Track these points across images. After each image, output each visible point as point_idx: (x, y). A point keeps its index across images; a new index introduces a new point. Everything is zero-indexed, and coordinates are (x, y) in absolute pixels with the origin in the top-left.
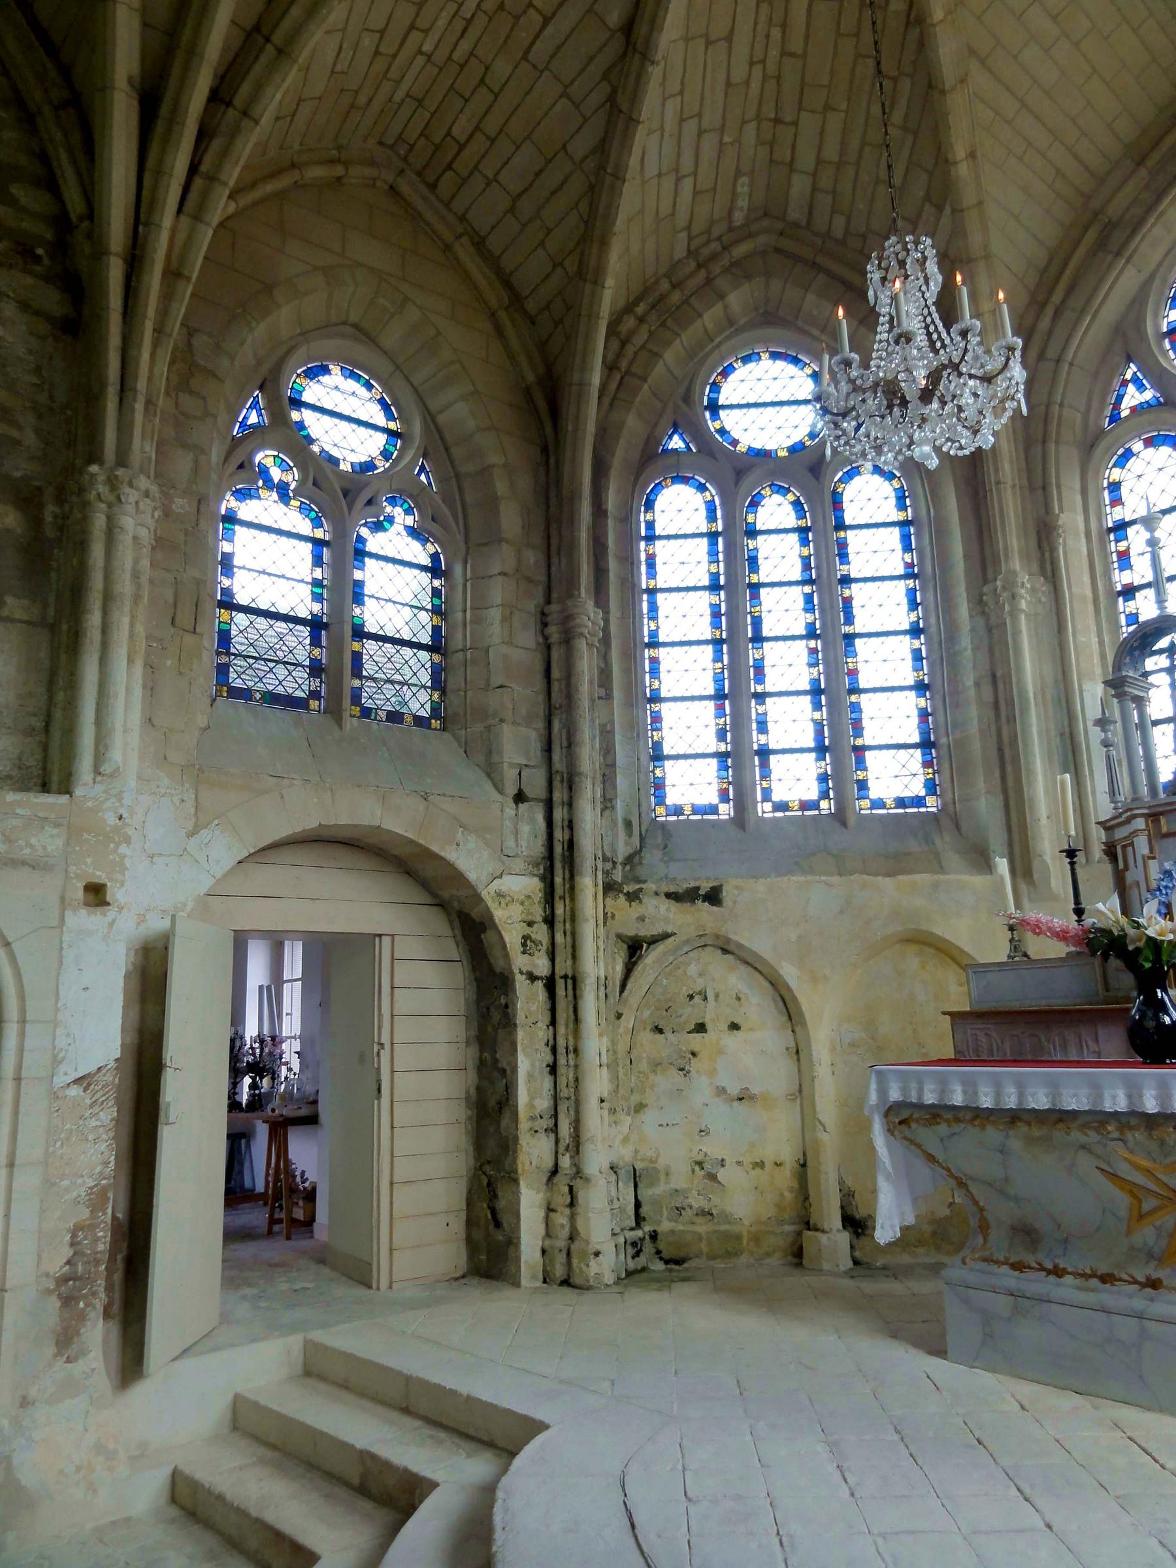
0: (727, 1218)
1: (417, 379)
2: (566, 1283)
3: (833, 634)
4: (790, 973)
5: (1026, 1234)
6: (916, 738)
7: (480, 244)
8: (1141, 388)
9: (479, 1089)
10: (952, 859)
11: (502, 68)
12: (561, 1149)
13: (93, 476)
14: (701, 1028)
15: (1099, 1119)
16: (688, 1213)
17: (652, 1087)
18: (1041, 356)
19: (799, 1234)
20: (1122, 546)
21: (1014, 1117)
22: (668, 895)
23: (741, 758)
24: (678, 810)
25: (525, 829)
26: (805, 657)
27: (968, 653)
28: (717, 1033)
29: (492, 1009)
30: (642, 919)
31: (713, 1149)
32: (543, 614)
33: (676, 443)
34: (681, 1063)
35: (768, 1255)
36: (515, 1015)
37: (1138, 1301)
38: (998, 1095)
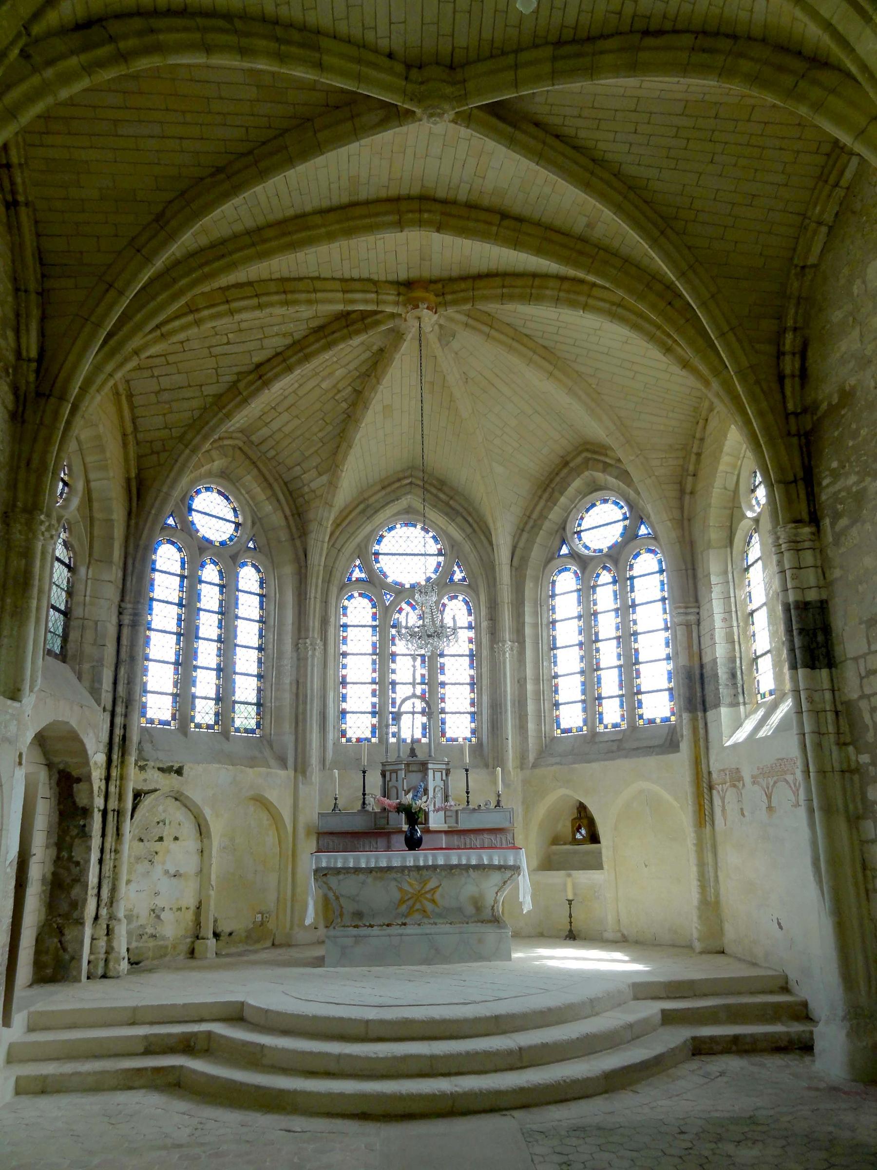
0: (164, 938)
1: (88, 459)
2: (104, 976)
3: (227, 642)
4: (208, 812)
5: (359, 915)
6: (255, 701)
7: (130, 396)
8: (361, 571)
9: (54, 874)
10: (272, 762)
11: (195, 344)
12: (103, 904)
13: (42, 522)
14: (161, 839)
15: (403, 869)
16: (145, 937)
17: (135, 871)
18: (333, 545)
19: (193, 942)
20: (345, 634)
21: (370, 870)
22: (159, 769)
23: (183, 699)
24: (151, 721)
25: (105, 726)
26: (215, 652)
27: (289, 667)
28: (168, 842)
29: (71, 827)
30: (145, 780)
31: (160, 902)
32: (120, 607)
33: (171, 521)
34: (150, 857)
35: (179, 954)
36: (91, 831)
37: (401, 930)
38: (368, 862)
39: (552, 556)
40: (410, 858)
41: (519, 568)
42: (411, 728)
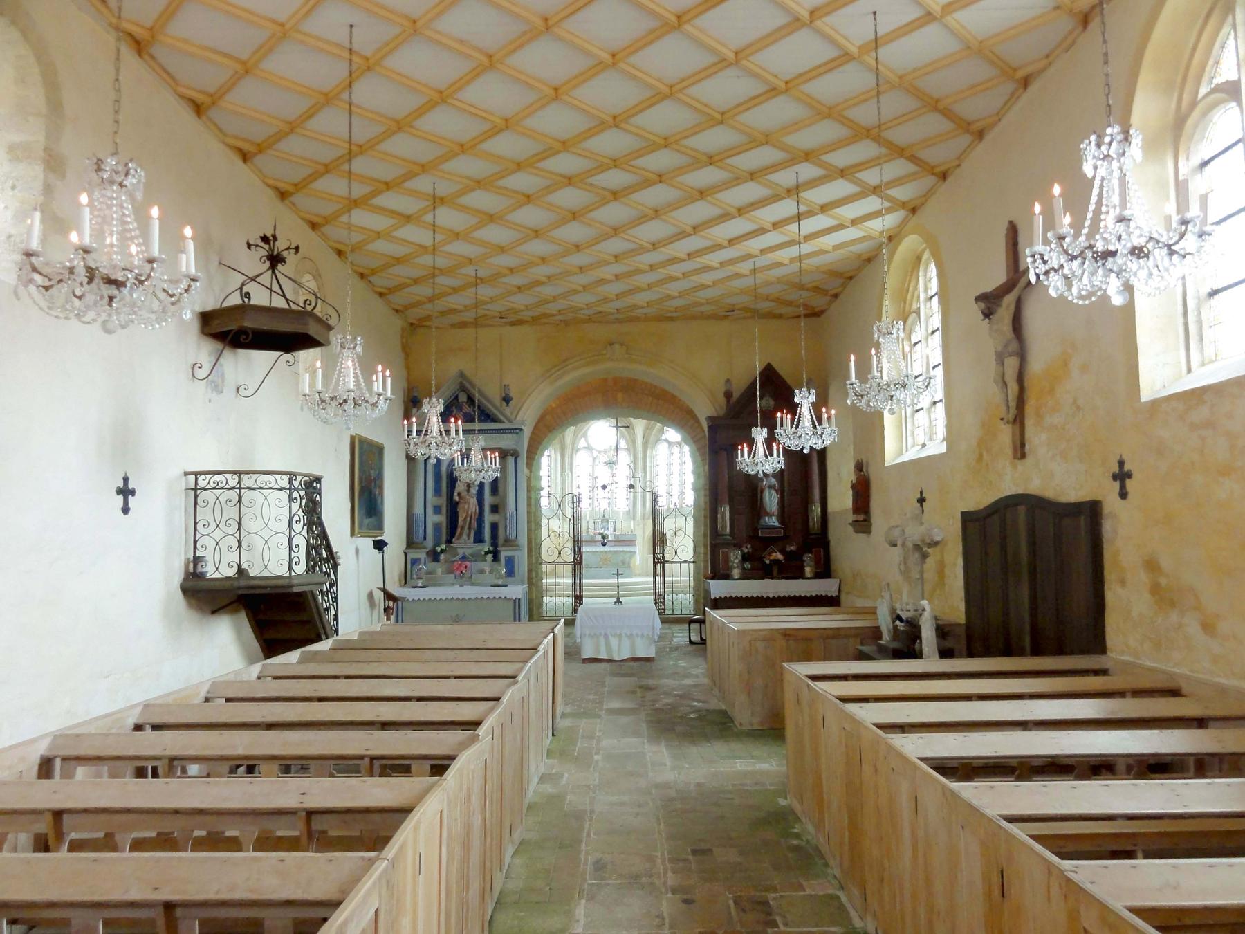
39: (658, 440)
40: (603, 548)
41: (645, 445)
42: (604, 505)
